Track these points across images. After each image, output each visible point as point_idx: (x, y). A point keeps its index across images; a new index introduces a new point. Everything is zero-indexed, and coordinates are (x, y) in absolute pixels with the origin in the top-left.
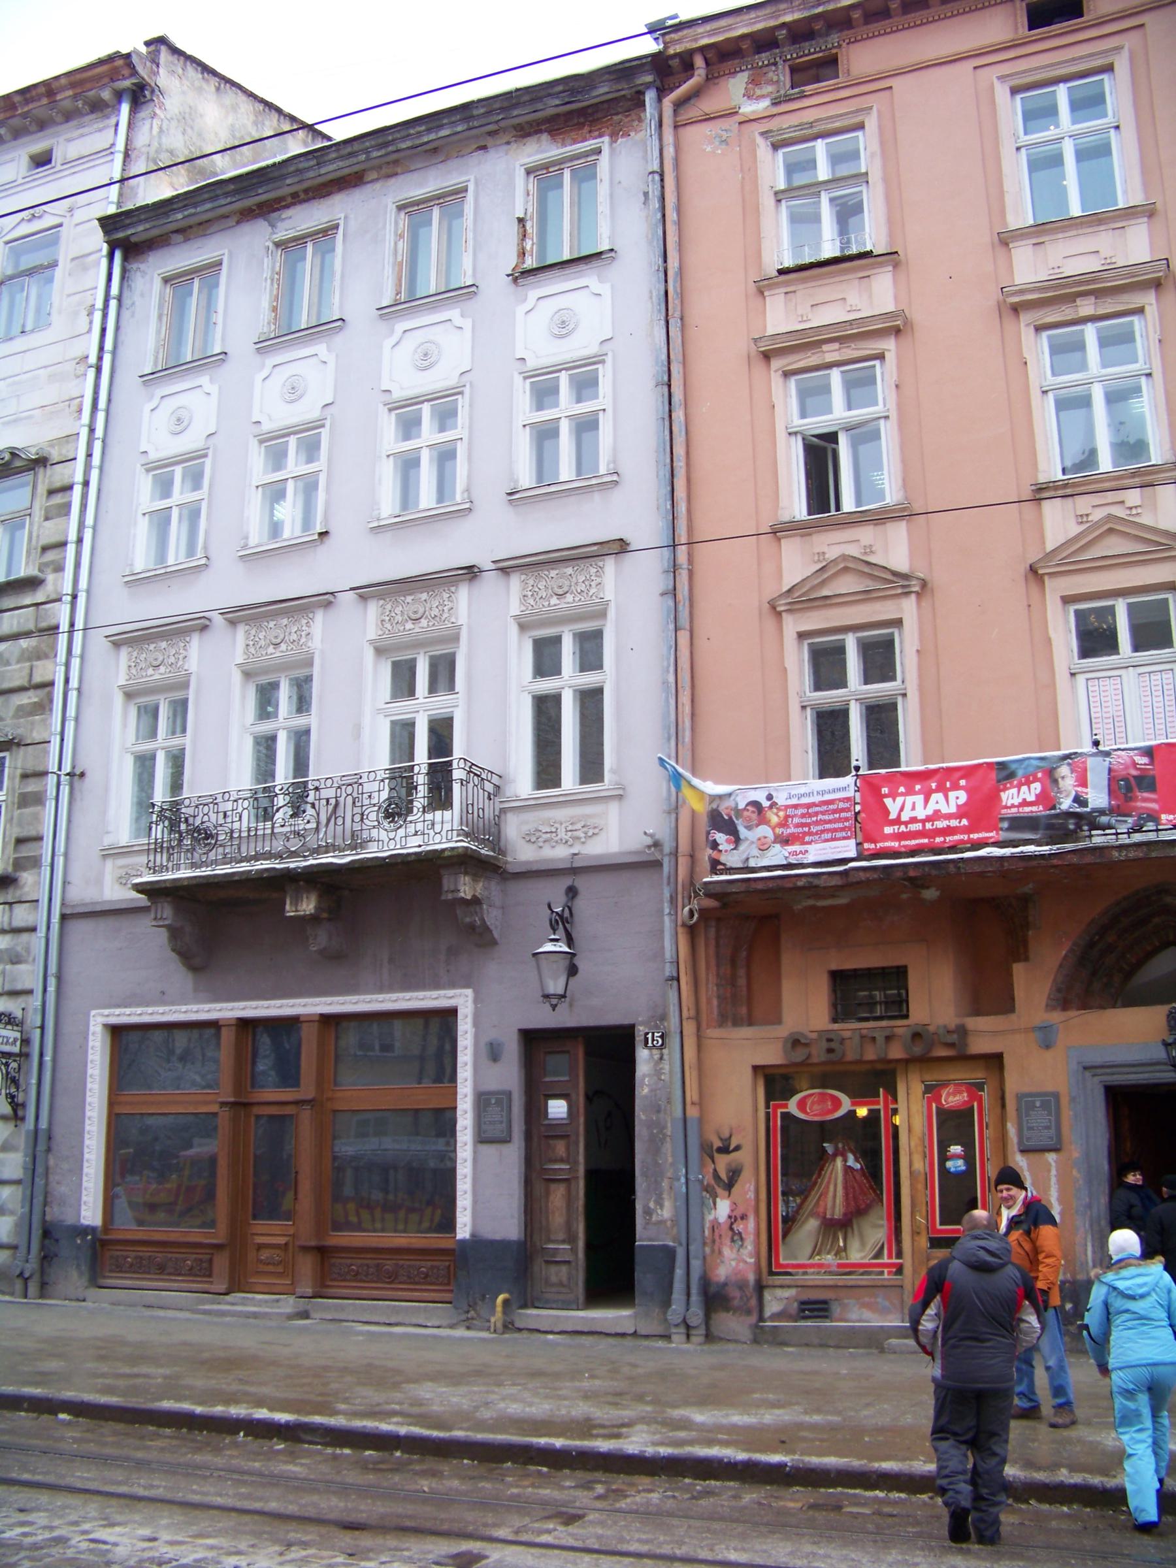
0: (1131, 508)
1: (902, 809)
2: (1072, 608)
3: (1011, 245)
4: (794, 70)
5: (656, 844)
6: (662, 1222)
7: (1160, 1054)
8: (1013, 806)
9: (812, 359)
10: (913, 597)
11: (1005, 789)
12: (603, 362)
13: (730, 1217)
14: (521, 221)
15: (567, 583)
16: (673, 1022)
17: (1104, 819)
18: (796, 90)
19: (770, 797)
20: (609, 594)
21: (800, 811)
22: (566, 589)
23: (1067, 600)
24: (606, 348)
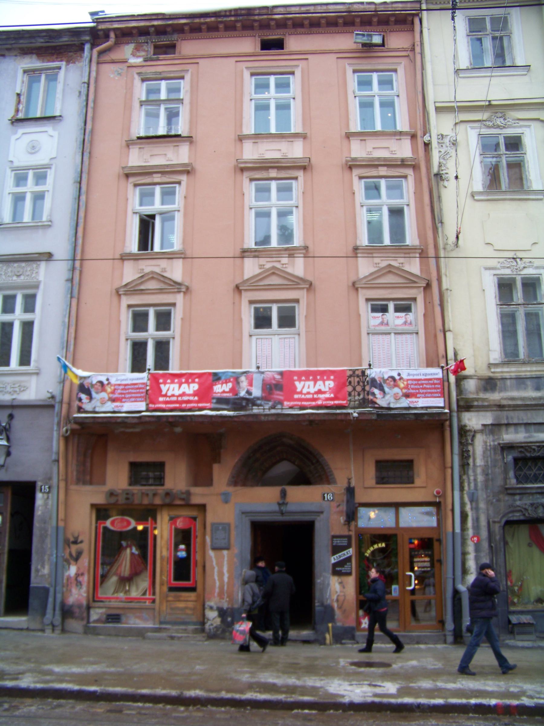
0: (283, 264)
1: (168, 390)
2: (253, 306)
3: (243, 141)
4: (156, 47)
5: (53, 397)
6: (43, 576)
7: (276, 508)
8: (218, 393)
9: (147, 180)
10: (182, 294)
11: (216, 385)
12: (50, 168)
13: (76, 574)
14: (19, 95)
15: (22, 270)
16: (55, 481)
17: (259, 402)
18: (155, 56)
19: (108, 380)
20: (41, 278)
21: (121, 387)
22: (20, 273)
23: (251, 302)
24: (53, 162)
